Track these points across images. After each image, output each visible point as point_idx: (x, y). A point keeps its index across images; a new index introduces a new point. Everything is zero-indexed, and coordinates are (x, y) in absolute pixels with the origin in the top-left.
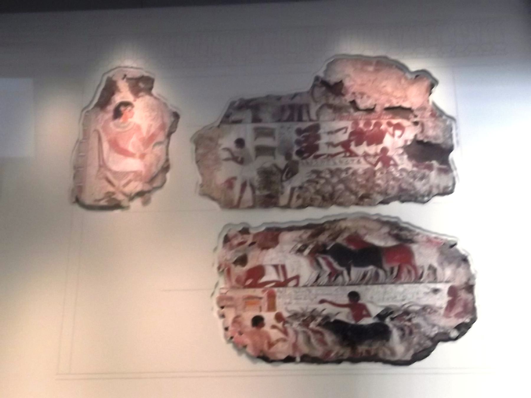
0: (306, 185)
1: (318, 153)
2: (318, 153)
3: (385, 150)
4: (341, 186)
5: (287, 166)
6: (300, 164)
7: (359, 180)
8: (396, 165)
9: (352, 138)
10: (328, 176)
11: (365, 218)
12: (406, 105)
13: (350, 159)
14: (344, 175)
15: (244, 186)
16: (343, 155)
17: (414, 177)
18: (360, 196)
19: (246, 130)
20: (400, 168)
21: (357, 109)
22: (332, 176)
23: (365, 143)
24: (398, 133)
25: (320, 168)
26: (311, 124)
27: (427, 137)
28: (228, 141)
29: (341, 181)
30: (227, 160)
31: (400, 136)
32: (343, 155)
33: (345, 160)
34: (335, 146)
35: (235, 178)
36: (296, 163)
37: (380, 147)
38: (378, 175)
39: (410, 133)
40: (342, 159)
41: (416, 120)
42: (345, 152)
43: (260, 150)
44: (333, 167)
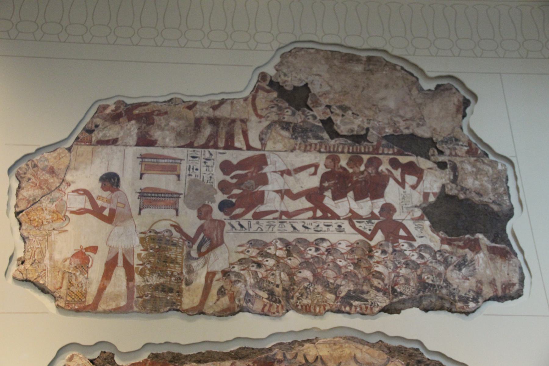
0: (237, 269)
1: (262, 208)
2: (262, 208)
4: (307, 274)
5: (201, 229)
6: (227, 228)
7: (342, 263)
8: (410, 238)
9: (326, 184)
10: (279, 253)
11: (357, 339)
12: (423, 132)
13: (322, 222)
14: (311, 252)
15: (110, 266)
16: (310, 214)
17: (446, 263)
19: (124, 160)
20: (416, 244)
21: (334, 134)
22: (289, 254)
23: (351, 194)
24: (411, 180)
25: (267, 238)
26: (251, 153)
27: (464, 189)
28: (86, 177)
29: (306, 264)
30: (80, 212)
31: (414, 187)
34: (295, 197)
35: (94, 249)
36: (221, 224)
37: (380, 202)
38: (377, 254)
39: (433, 182)
41: (441, 159)
42: (314, 210)
43: (150, 198)
44: (291, 238)
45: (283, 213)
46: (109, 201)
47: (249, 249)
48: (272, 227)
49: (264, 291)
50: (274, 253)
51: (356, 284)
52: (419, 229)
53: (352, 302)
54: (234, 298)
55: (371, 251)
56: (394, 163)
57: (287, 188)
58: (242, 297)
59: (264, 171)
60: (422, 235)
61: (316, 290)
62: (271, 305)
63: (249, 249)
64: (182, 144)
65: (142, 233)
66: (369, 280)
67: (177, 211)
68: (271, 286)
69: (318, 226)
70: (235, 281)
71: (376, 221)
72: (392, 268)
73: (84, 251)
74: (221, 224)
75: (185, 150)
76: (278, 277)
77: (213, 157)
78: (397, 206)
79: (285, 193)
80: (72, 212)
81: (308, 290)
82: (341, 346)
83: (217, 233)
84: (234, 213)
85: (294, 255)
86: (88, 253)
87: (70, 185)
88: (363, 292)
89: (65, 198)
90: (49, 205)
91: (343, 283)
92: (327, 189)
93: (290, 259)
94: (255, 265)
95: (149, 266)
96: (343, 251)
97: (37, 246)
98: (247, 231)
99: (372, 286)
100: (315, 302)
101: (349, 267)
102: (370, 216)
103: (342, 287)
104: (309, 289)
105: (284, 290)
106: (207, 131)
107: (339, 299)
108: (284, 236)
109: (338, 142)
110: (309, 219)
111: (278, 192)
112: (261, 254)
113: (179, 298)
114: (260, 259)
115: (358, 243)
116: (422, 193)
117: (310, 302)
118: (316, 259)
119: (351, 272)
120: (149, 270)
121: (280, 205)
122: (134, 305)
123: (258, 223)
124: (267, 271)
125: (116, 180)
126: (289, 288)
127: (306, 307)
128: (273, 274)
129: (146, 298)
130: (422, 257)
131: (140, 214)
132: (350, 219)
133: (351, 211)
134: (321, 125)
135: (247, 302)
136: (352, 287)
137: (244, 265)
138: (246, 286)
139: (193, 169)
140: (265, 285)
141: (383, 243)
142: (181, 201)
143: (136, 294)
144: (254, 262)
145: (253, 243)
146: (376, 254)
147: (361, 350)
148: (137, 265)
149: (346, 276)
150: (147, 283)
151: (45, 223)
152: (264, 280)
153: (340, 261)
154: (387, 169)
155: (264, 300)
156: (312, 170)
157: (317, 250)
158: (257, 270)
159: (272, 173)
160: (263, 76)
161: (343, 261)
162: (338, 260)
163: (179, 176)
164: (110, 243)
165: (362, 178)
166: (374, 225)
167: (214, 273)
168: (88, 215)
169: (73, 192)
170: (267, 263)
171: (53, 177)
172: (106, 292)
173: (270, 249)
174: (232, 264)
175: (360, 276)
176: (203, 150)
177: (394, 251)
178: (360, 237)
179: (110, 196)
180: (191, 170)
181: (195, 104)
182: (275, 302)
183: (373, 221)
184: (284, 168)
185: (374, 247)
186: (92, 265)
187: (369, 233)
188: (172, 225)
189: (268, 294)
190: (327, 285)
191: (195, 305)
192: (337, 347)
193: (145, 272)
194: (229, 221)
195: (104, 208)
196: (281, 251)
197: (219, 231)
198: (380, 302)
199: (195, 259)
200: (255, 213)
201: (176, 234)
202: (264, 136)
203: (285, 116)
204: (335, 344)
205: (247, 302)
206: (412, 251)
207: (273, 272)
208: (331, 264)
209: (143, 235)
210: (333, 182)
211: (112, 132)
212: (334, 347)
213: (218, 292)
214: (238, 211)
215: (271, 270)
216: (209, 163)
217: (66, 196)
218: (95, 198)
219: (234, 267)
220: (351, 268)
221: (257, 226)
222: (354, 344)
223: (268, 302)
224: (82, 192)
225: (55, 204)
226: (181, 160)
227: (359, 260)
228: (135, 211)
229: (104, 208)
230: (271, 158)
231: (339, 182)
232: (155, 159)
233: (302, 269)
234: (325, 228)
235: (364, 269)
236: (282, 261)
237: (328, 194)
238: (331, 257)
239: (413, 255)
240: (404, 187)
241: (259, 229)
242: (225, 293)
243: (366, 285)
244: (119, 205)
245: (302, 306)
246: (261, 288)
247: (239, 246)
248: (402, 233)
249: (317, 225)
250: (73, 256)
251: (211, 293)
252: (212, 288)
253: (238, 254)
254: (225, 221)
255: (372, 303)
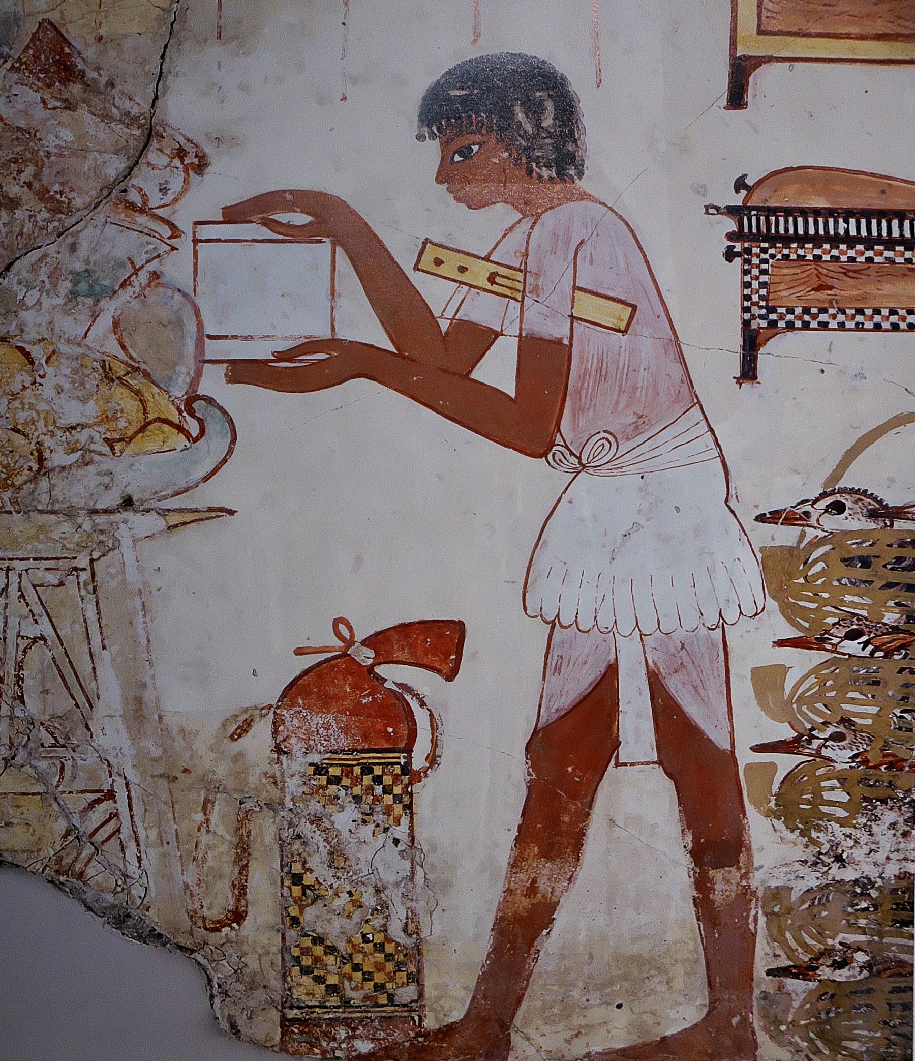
35: (439, 643)
65: (773, 517)
73: (365, 656)
80: (243, 371)
86: (394, 674)
87: (201, 166)
89: (177, 267)
90: (72, 326)
95: (841, 756)
120: (843, 780)
122: (756, 1022)
129: (841, 975)
131: (748, 372)
143: (765, 955)
150: (836, 872)
151: (58, 458)
164: (548, 595)
168: (362, 391)
169: (232, 215)
186: (433, 760)
193: (818, 800)
217: (185, 245)
224: (300, 219)
225: (110, 309)
244: (587, 307)
250: (294, 691)
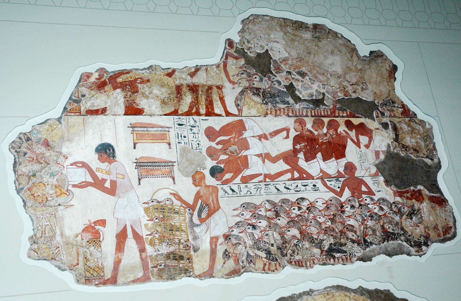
0: (236, 232)
1: (247, 172)
2: (247, 172)
3: (350, 168)
4: (295, 232)
5: (198, 196)
6: (221, 193)
7: (321, 220)
8: (370, 193)
9: (298, 147)
12: (367, 96)
16: (289, 175)
17: (399, 212)
18: (325, 249)
19: (115, 128)
20: (376, 198)
21: (297, 99)
22: (277, 215)
23: (319, 155)
24: (364, 139)
25: (257, 201)
26: (230, 119)
27: (405, 147)
29: (292, 222)
31: (367, 146)
32: (289, 175)
33: (292, 185)
34: (274, 160)
35: (103, 223)
36: (215, 189)
37: (343, 162)
38: (348, 209)
39: (382, 141)
40: (288, 183)
41: (385, 120)
42: (291, 171)
43: (146, 167)
44: (277, 199)
45: (266, 176)
46: (108, 173)
47: (243, 213)
48: (259, 189)
49: (262, 251)
50: (265, 214)
51: (335, 238)
52: (376, 184)
53: (334, 254)
54: (238, 260)
55: (342, 207)
56: (349, 124)
57: (266, 152)
58: (244, 258)
59: (244, 136)
60: (379, 190)
61: (304, 246)
62: (270, 264)
63: (243, 213)
64: (168, 112)
65: (145, 203)
66: (345, 233)
67: (174, 179)
68: (267, 245)
69: (297, 186)
70: (236, 244)
71: (342, 179)
72: (361, 221)
73: (93, 225)
74: (215, 189)
75: (171, 117)
76: (272, 237)
77: (197, 124)
78: (357, 164)
79: (265, 157)
80: (74, 186)
81: (298, 247)
82: (334, 295)
83: (213, 199)
84: (224, 179)
85: (282, 216)
86: (97, 227)
87: (67, 158)
88: (341, 245)
89: (65, 172)
90: (50, 180)
91: (325, 237)
92: (299, 151)
93: (279, 220)
94: (251, 227)
95: (157, 236)
96: (321, 209)
97: (47, 224)
98: (238, 195)
99: (347, 238)
100: (305, 257)
101: (327, 223)
102: (337, 174)
103: (324, 242)
104: (299, 245)
105: (279, 248)
106: (188, 99)
107: (324, 253)
108: (272, 198)
109: (301, 106)
110: (289, 180)
111: (259, 155)
112: (254, 216)
113: (190, 265)
114: (254, 221)
115: (331, 200)
116: (374, 152)
117: (301, 257)
118: (300, 218)
119: (329, 227)
120: (158, 239)
121: (263, 169)
122: (150, 275)
123: (247, 186)
124: (261, 232)
125: (111, 151)
126: (283, 246)
127: (298, 262)
128: (267, 235)
129: (161, 267)
130: (382, 209)
131: (139, 184)
132: (322, 179)
133: (322, 171)
134: (285, 90)
135: (249, 263)
136: (332, 241)
137: (242, 228)
138: (246, 248)
139: (181, 136)
140: (262, 246)
141: (350, 198)
142: (176, 168)
143: (150, 265)
144: (249, 224)
145: (245, 206)
146: (347, 209)
147: (349, 297)
148: (147, 235)
149: (326, 231)
150: (158, 252)
151: (49, 199)
152: (260, 241)
153: (320, 218)
154: (344, 131)
155: (263, 259)
156: (285, 133)
157: (300, 209)
158: (253, 232)
159: (252, 138)
160: (230, 43)
161: (322, 217)
162: (318, 217)
163: (169, 144)
164: (117, 215)
165: (326, 140)
166: (341, 183)
167: (217, 238)
168: (90, 188)
169: (71, 165)
170: (259, 224)
171: (49, 150)
172: (121, 265)
173: (261, 211)
174: (231, 228)
175: (337, 231)
176: (187, 117)
177: (360, 205)
178: (332, 195)
179: (108, 167)
180: (180, 138)
181: (174, 71)
182: (272, 260)
183: (340, 179)
184: (260, 133)
185: (344, 203)
186: (103, 239)
187: (339, 190)
188: (171, 194)
189: (266, 254)
190: (312, 240)
191: (205, 270)
192: (330, 296)
193: (155, 242)
194: (222, 186)
195: (104, 181)
196: (270, 212)
197: (214, 196)
198: (357, 253)
199: (198, 225)
200: (242, 176)
201: (177, 203)
202: (239, 102)
203: (254, 82)
204: (328, 294)
205: (249, 263)
206: (374, 204)
207: (267, 232)
208: (313, 221)
209: (146, 206)
210: (303, 144)
211: (99, 100)
212: (328, 297)
213: (223, 256)
214: (228, 176)
215: (265, 230)
216: (195, 130)
217: (65, 169)
218: (94, 170)
219: (233, 231)
220: (329, 223)
221: (246, 190)
222: (343, 292)
223: (267, 261)
224: (80, 165)
225: (56, 178)
226: (169, 128)
227: (334, 215)
228: (135, 181)
229: (104, 181)
230: (248, 123)
231: (309, 145)
232: (145, 127)
233: (290, 228)
234: (303, 188)
235: (340, 224)
236: (272, 221)
237: (301, 155)
238: (312, 215)
239: (375, 208)
240: (359, 147)
241: (249, 193)
242: (229, 256)
243: (343, 238)
244: (118, 176)
245: (295, 262)
246: (259, 249)
247: (234, 210)
248: (364, 189)
249: (296, 185)
250: (84, 230)
251: (217, 257)
252: (218, 252)
253: (234, 218)
254: (218, 186)
255: (350, 254)
